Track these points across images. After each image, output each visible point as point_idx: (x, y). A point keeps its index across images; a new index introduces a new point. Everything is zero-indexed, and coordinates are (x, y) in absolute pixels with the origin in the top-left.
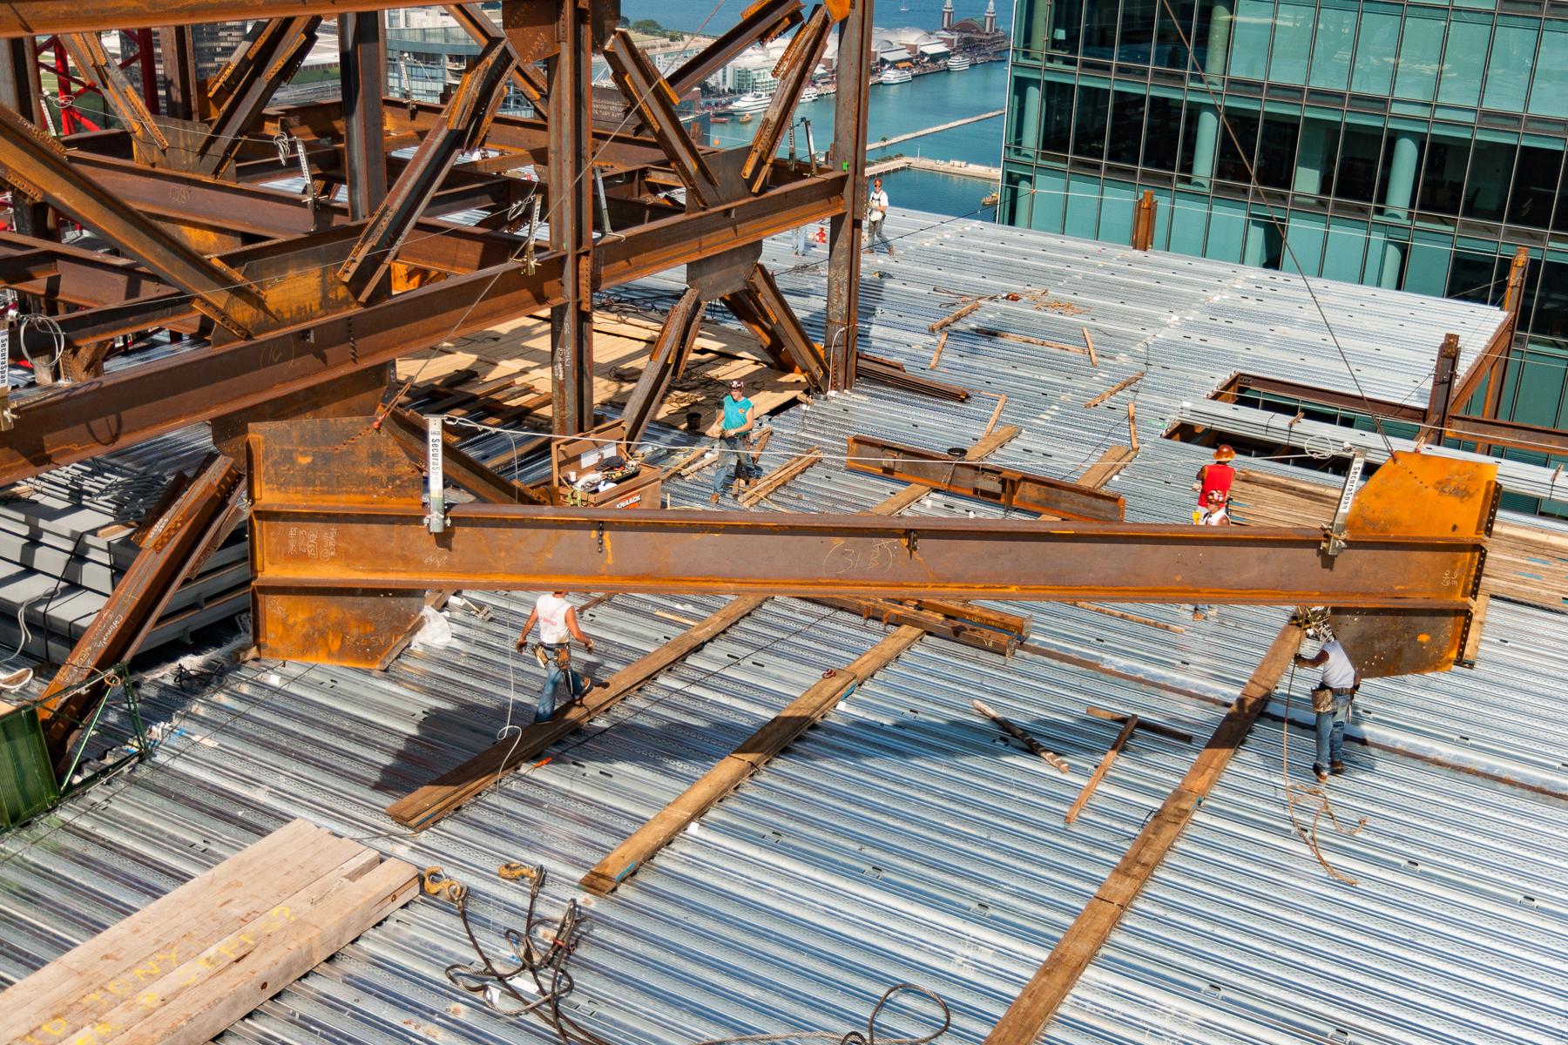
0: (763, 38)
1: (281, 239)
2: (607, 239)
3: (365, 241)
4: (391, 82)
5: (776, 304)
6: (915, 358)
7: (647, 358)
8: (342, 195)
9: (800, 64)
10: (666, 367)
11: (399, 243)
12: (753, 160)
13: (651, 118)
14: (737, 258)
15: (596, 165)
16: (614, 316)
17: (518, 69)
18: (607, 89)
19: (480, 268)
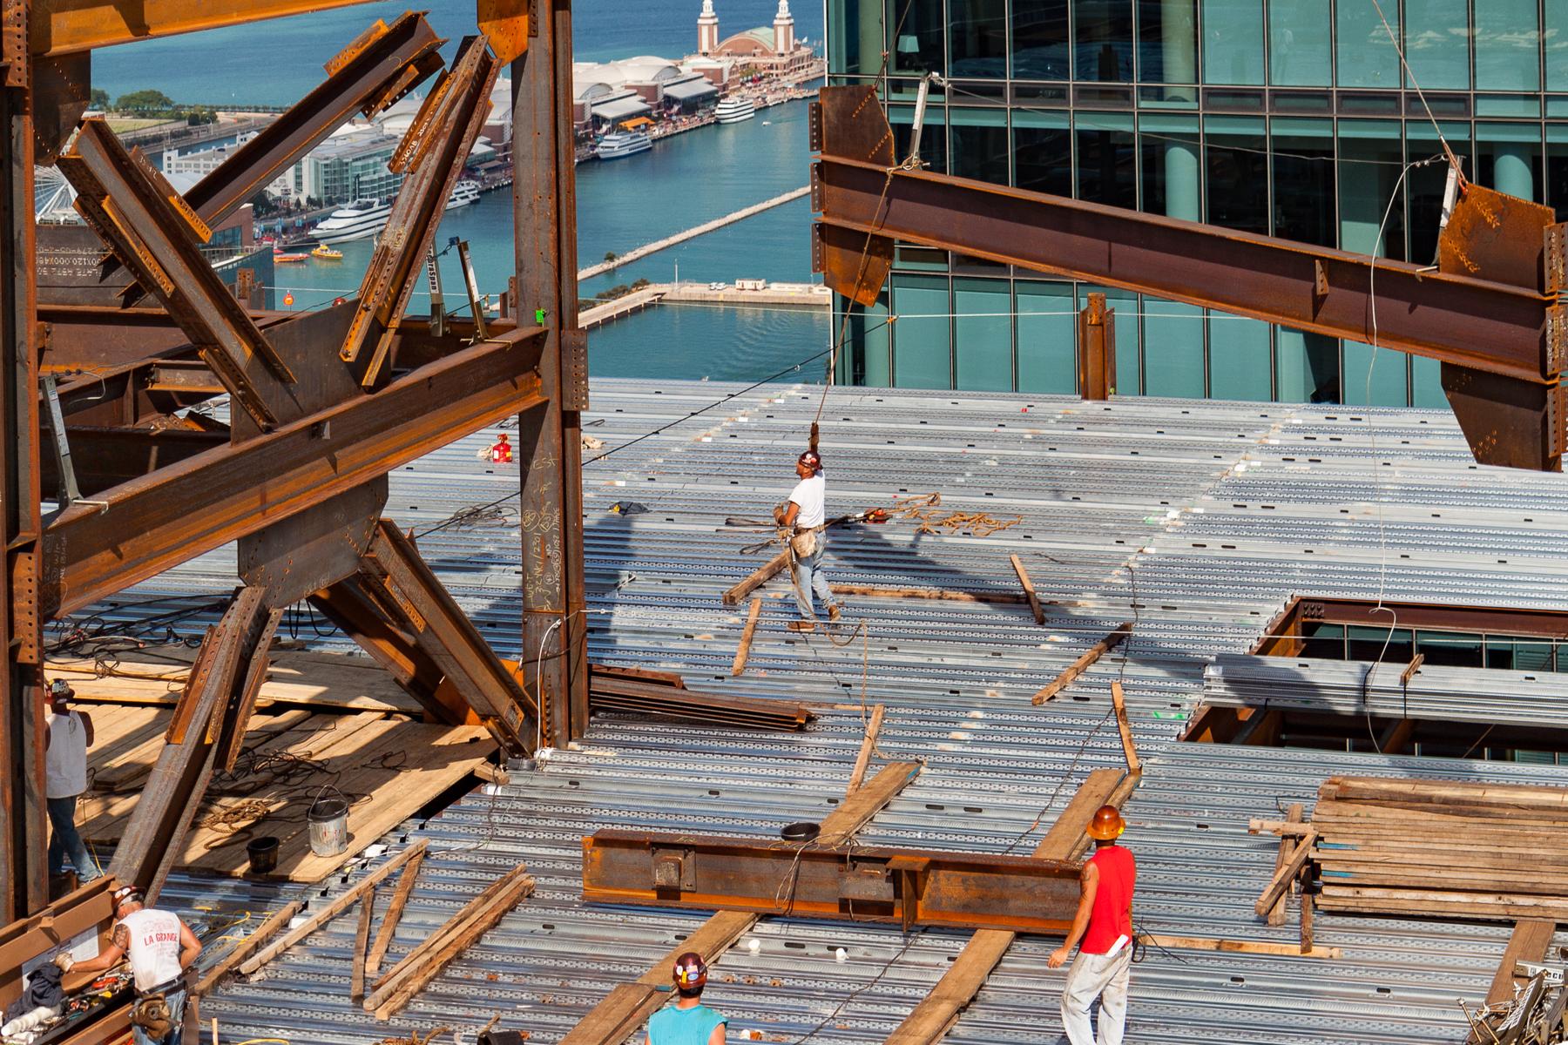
2: (73, 512)
5: (420, 593)
6: (698, 658)
7: (160, 740)
9: (442, 143)
10: (201, 751)
14: (339, 516)
16: (90, 664)
18: (69, 226)
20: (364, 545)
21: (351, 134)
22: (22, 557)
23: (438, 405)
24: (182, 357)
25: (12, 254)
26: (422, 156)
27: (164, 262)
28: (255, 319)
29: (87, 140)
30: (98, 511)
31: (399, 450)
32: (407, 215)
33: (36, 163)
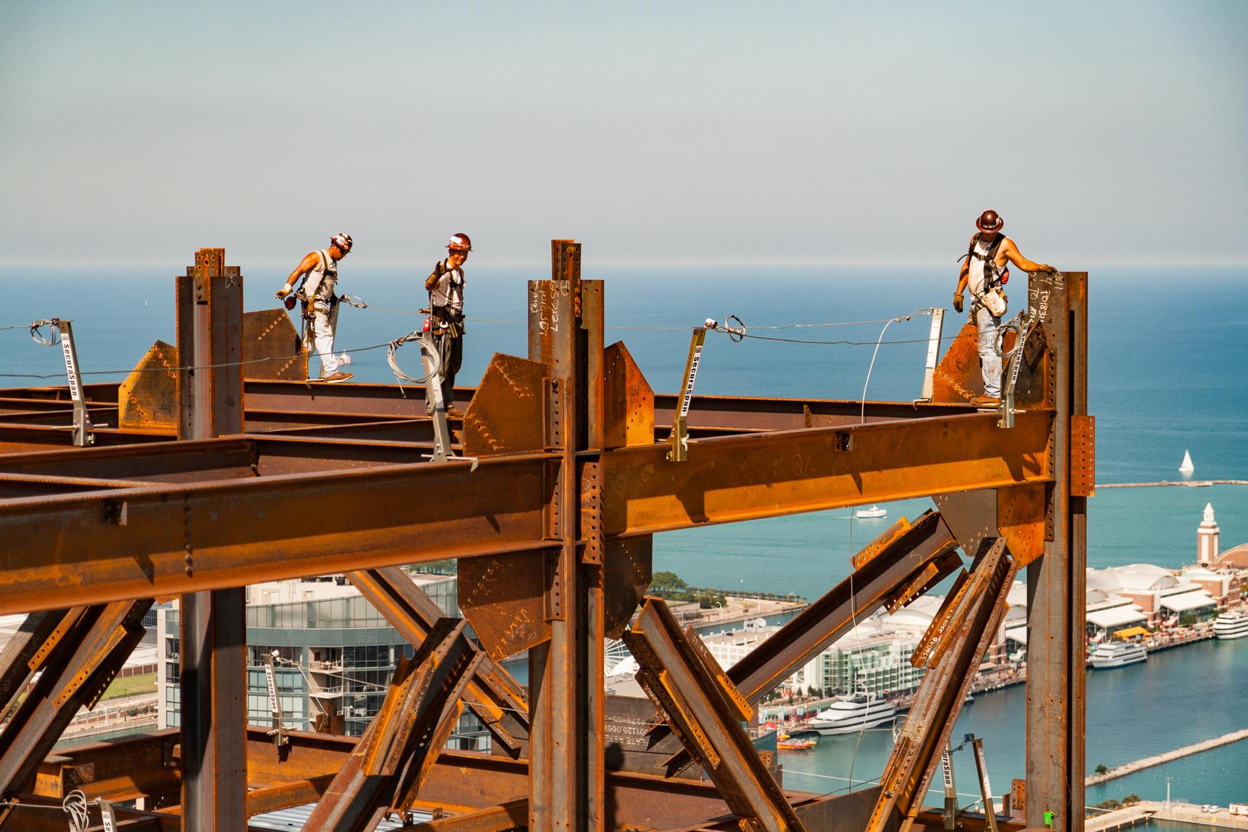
0: (891, 598)
9: (961, 642)
13: (704, 745)
26: (940, 655)
27: (711, 735)
32: (927, 709)
33: (606, 635)
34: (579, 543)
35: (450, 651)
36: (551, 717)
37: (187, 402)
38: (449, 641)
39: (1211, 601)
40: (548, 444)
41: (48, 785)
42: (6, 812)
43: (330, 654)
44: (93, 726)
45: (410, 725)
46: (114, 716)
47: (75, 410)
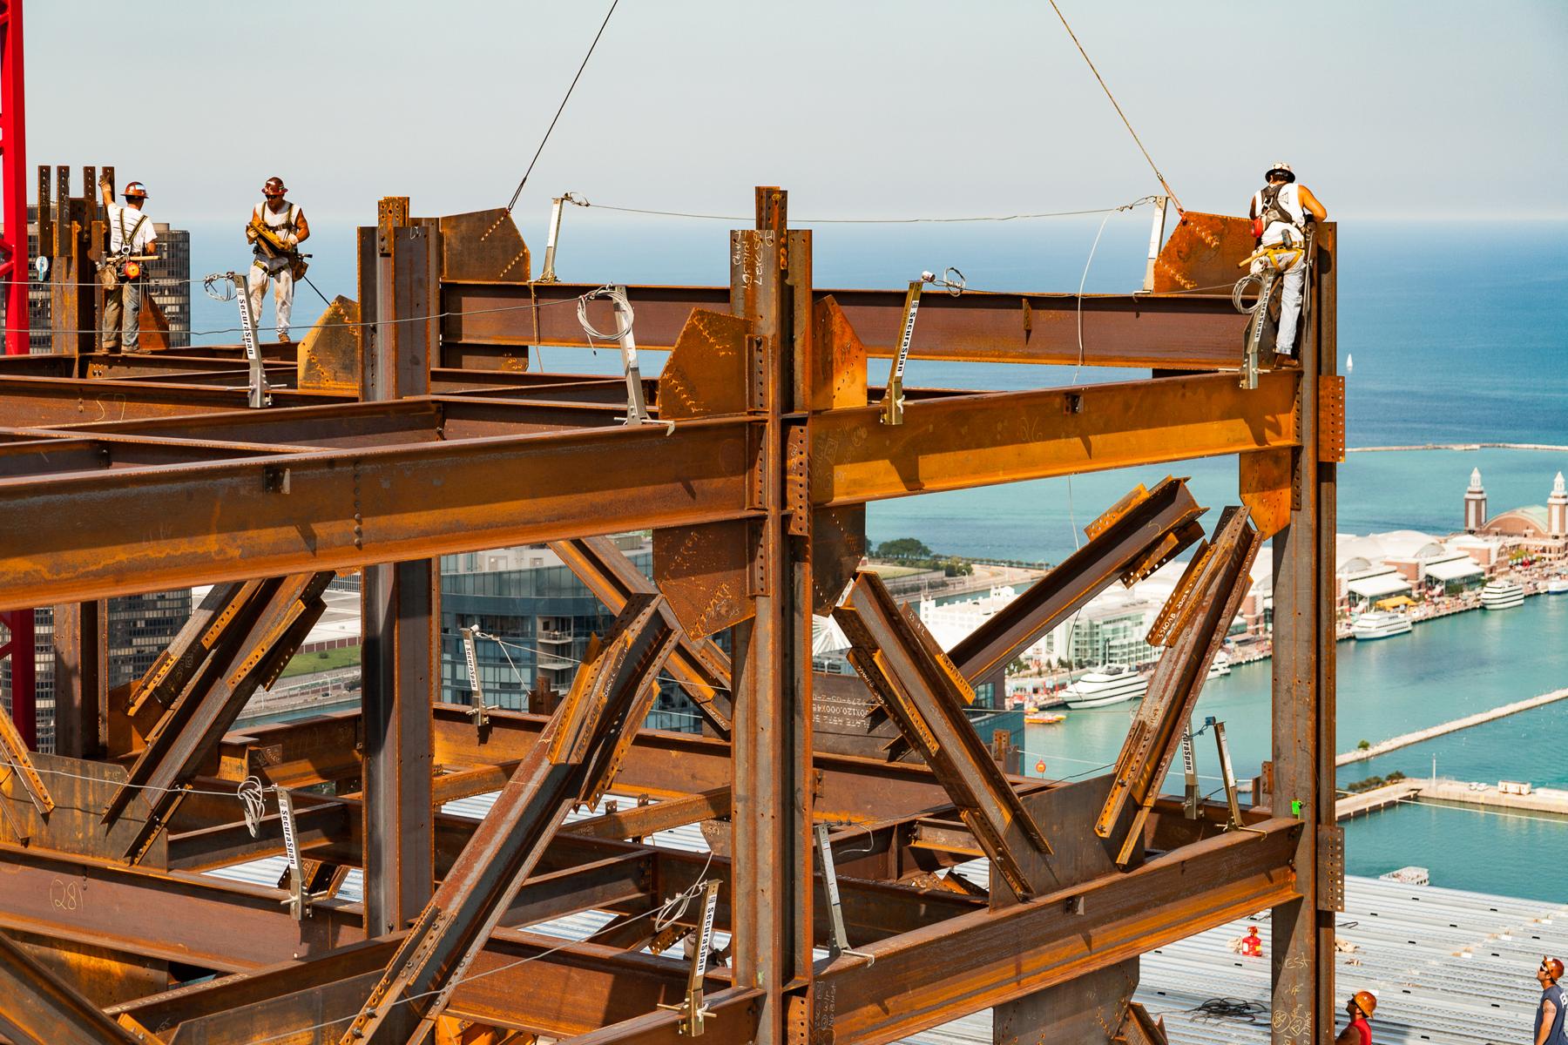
1: (243, 974)
2: (845, 961)
3: (393, 977)
4: (447, 671)
8: (353, 884)
9: (1200, 618)
11: (455, 980)
12: (1115, 804)
13: (922, 730)
14: (1091, 995)
15: (819, 817)
17: (680, 649)
19: (608, 1021)
20: (1115, 1028)
21: (1113, 596)
22: (796, 1001)
23: (1192, 892)
24: (944, 817)
25: (793, 701)
26: (1180, 630)
28: (1013, 784)
29: (860, 593)
30: (865, 963)
31: (1151, 933)
34: (785, 512)
35: (644, 630)
36: (755, 701)
37: (370, 361)
38: (643, 618)
39: (1479, 570)
40: (751, 405)
41: (233, 770)
42: (179, 799)
43: (562, 624)
44: (273, 705)
45: (601, 709)
46: (338, 687)
47: (251, 370)
